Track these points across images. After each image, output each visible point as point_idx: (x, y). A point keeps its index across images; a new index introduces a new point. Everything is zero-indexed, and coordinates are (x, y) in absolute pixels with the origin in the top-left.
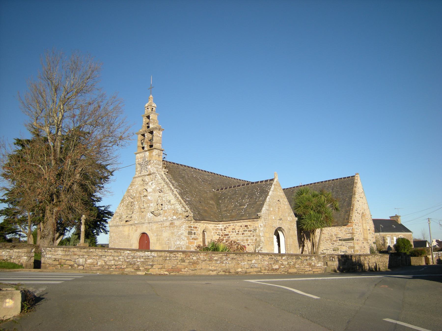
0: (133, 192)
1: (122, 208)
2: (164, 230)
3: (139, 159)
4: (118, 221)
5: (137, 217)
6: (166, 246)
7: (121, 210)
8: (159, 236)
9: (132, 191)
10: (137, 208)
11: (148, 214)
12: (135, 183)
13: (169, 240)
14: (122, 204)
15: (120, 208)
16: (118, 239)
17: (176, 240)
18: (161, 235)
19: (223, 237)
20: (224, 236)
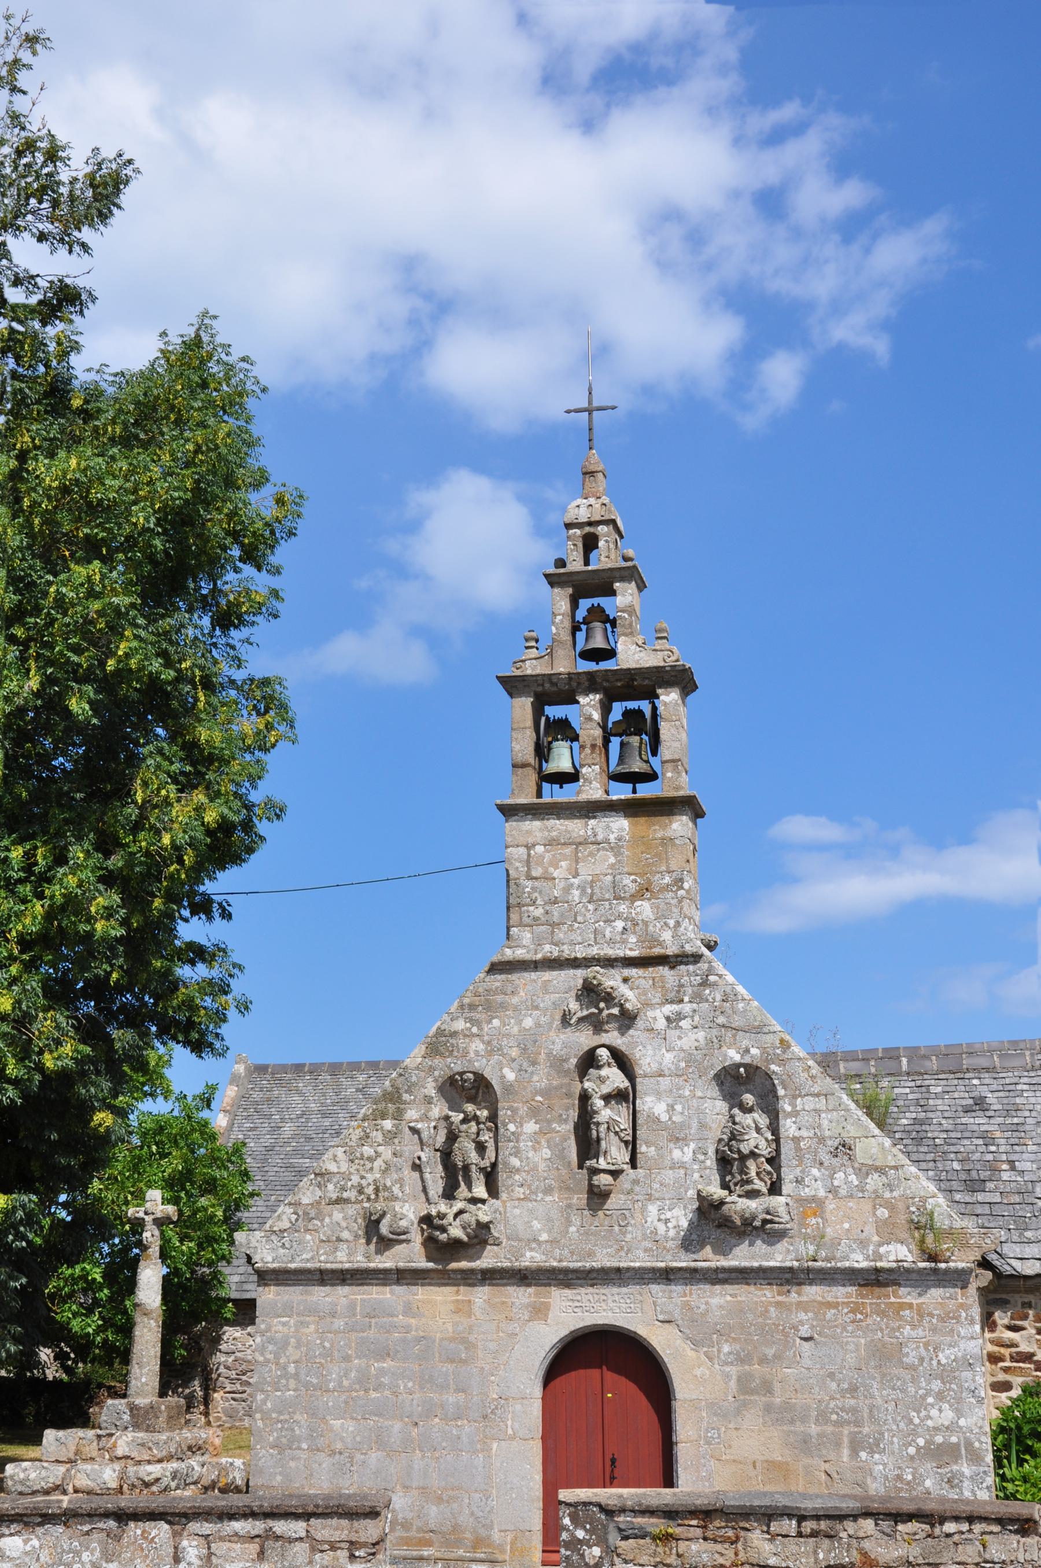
0: (490, 1053)
1: (386, 1152)
2: (802, 1323)
3: (540, 849)
4: (346, 1235)
5: (536, 1225)
6: (829, 1429)
7: (378, 1163)
8: (763, 1360)
9: (477, 1046)
10: (542, 1166)
11: (653, 1209)
12: (515, 1000)
13: (853, 1390)
14: (388, 1124)
15: (368, 1151)
16: (347, 1359)
17: (924, 1398)
18: (778, 1357)
19: (1006, 1370)
20: (1007, 1364)
